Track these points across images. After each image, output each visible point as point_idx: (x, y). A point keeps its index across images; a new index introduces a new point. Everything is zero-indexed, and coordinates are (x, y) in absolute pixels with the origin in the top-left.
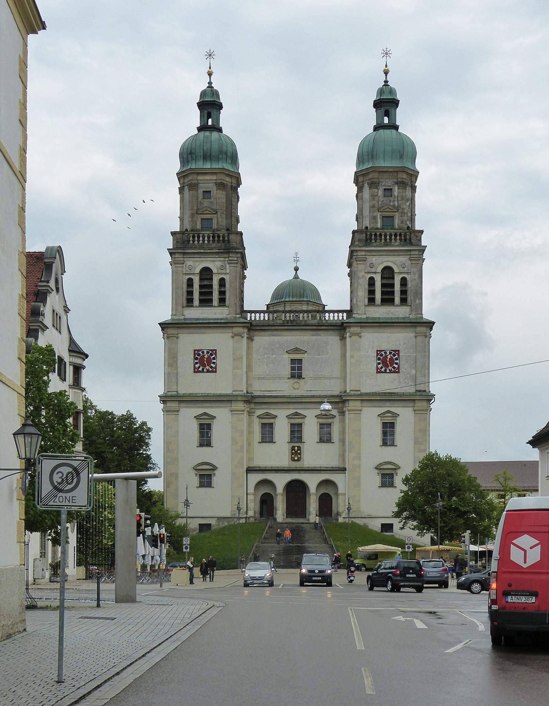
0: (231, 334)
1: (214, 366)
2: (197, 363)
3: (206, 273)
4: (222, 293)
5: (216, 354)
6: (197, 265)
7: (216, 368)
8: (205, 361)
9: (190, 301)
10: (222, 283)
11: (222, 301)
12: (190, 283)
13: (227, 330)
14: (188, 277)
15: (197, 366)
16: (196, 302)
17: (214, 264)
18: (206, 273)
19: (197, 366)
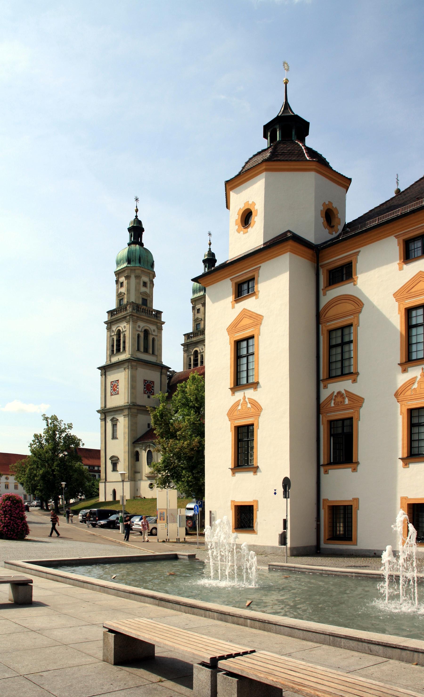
0: (123, 369)
4: (124, 342)
6: (114, 328)
9: (113, 351)
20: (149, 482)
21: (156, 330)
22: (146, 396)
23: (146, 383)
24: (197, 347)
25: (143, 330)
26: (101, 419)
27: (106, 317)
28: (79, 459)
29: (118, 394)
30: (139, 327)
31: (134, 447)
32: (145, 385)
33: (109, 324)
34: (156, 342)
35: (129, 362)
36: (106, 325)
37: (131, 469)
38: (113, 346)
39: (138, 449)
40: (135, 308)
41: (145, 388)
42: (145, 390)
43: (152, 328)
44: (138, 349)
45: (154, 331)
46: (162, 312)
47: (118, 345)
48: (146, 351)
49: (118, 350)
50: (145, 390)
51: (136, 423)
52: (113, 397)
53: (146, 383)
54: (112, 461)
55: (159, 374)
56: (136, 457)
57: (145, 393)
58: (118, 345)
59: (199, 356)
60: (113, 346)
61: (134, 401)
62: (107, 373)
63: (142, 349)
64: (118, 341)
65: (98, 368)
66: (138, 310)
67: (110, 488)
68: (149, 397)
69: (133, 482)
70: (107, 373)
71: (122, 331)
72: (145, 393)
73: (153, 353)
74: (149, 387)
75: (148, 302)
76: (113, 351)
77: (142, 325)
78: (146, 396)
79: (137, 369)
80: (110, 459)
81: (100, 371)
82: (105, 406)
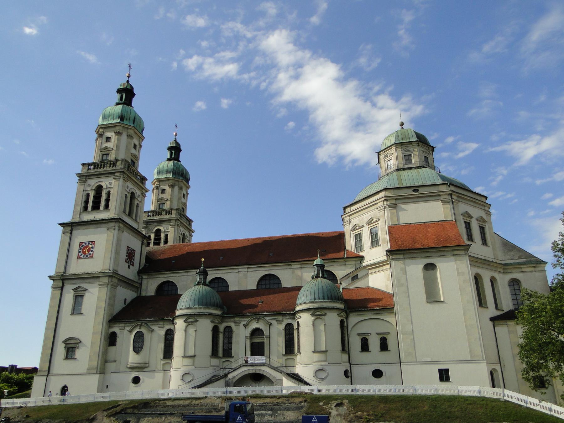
0: (106, 229)
1: (91, 252)
2: (80, 252)
3: (99, 189)
4: (108, 200)
5: (94, 244)
6: (93, 183)
7: (93, 255)
8: (86, 250)
10: (109, 194)
11: (107, 206)
12: (88, 195)
13: (103, 225)
14: (87, 192)
15: (80, 254)
17: (105, 182)
18: (99, 189)
19: (80, 254)
20: (134, 374)
21: (141, 196)
22: (127, 265)
24: (161, 226)
25: (130, 192)
26: (54, 288)
27: (79, 169)
29: (92, 257)
30: (128, 187)
31: (110, 327)
33: (83, 178)
34: (139, 208)
35: (116, 222)
36: (79, 178)
37: (102, 357)
38: (87, 202)
39: (116, 329)
40: (127, 166)
43: (138, 192)
44: (124, 212)
45: (139, 196)
46: (146, 180)
48: (130, 215)
49: (96, 207)
51: (115, 296)
52: (80, 260)
54: (66, 344)
55: (140, 243)
56: (112, 339)
57: (126, 262)
59: (163, 236)
60: (87, 202)
61: (116, 269)
62: (74, 232)
63: (127, 212)
65: (60, 224)
66: (128, 170)
67: (56, 385)
68: (129, 267)
69: (102, 375)
70: (74, 232)
72: (126, 262)
74: (130, 254)
75: (136, 164)
76: (85, 208)
77: (131, 187)
78: (127, 265)
79: (123, 232)
80: (65, 342)
81: (62, 228)
82: (65, 272)
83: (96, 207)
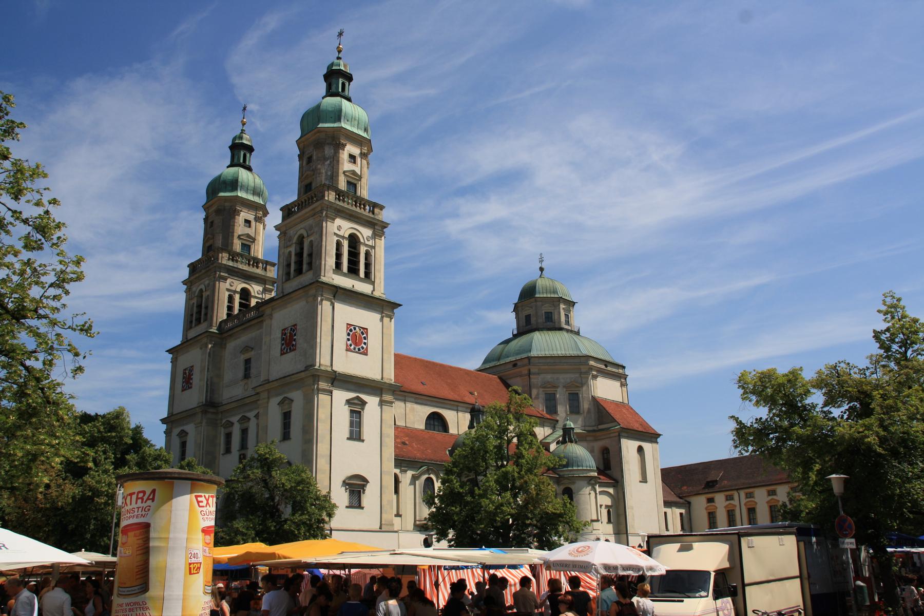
16: (292, 276)
23: (351, 330)
25: (347, 236)
28: (98, 497)
30: (339, 228)
32: (349, 334)
41: (348, 340)
42: (349, 342)
47: (299, 263)
48: (353, 270)
50: (349, 342)
53: (351, 330)
58: (299, 263)
60: (289, 265)
64: (300, 255)
71: (305, 235)
73: (367, 274)
76: (288, 274)
83: (299, 271)
